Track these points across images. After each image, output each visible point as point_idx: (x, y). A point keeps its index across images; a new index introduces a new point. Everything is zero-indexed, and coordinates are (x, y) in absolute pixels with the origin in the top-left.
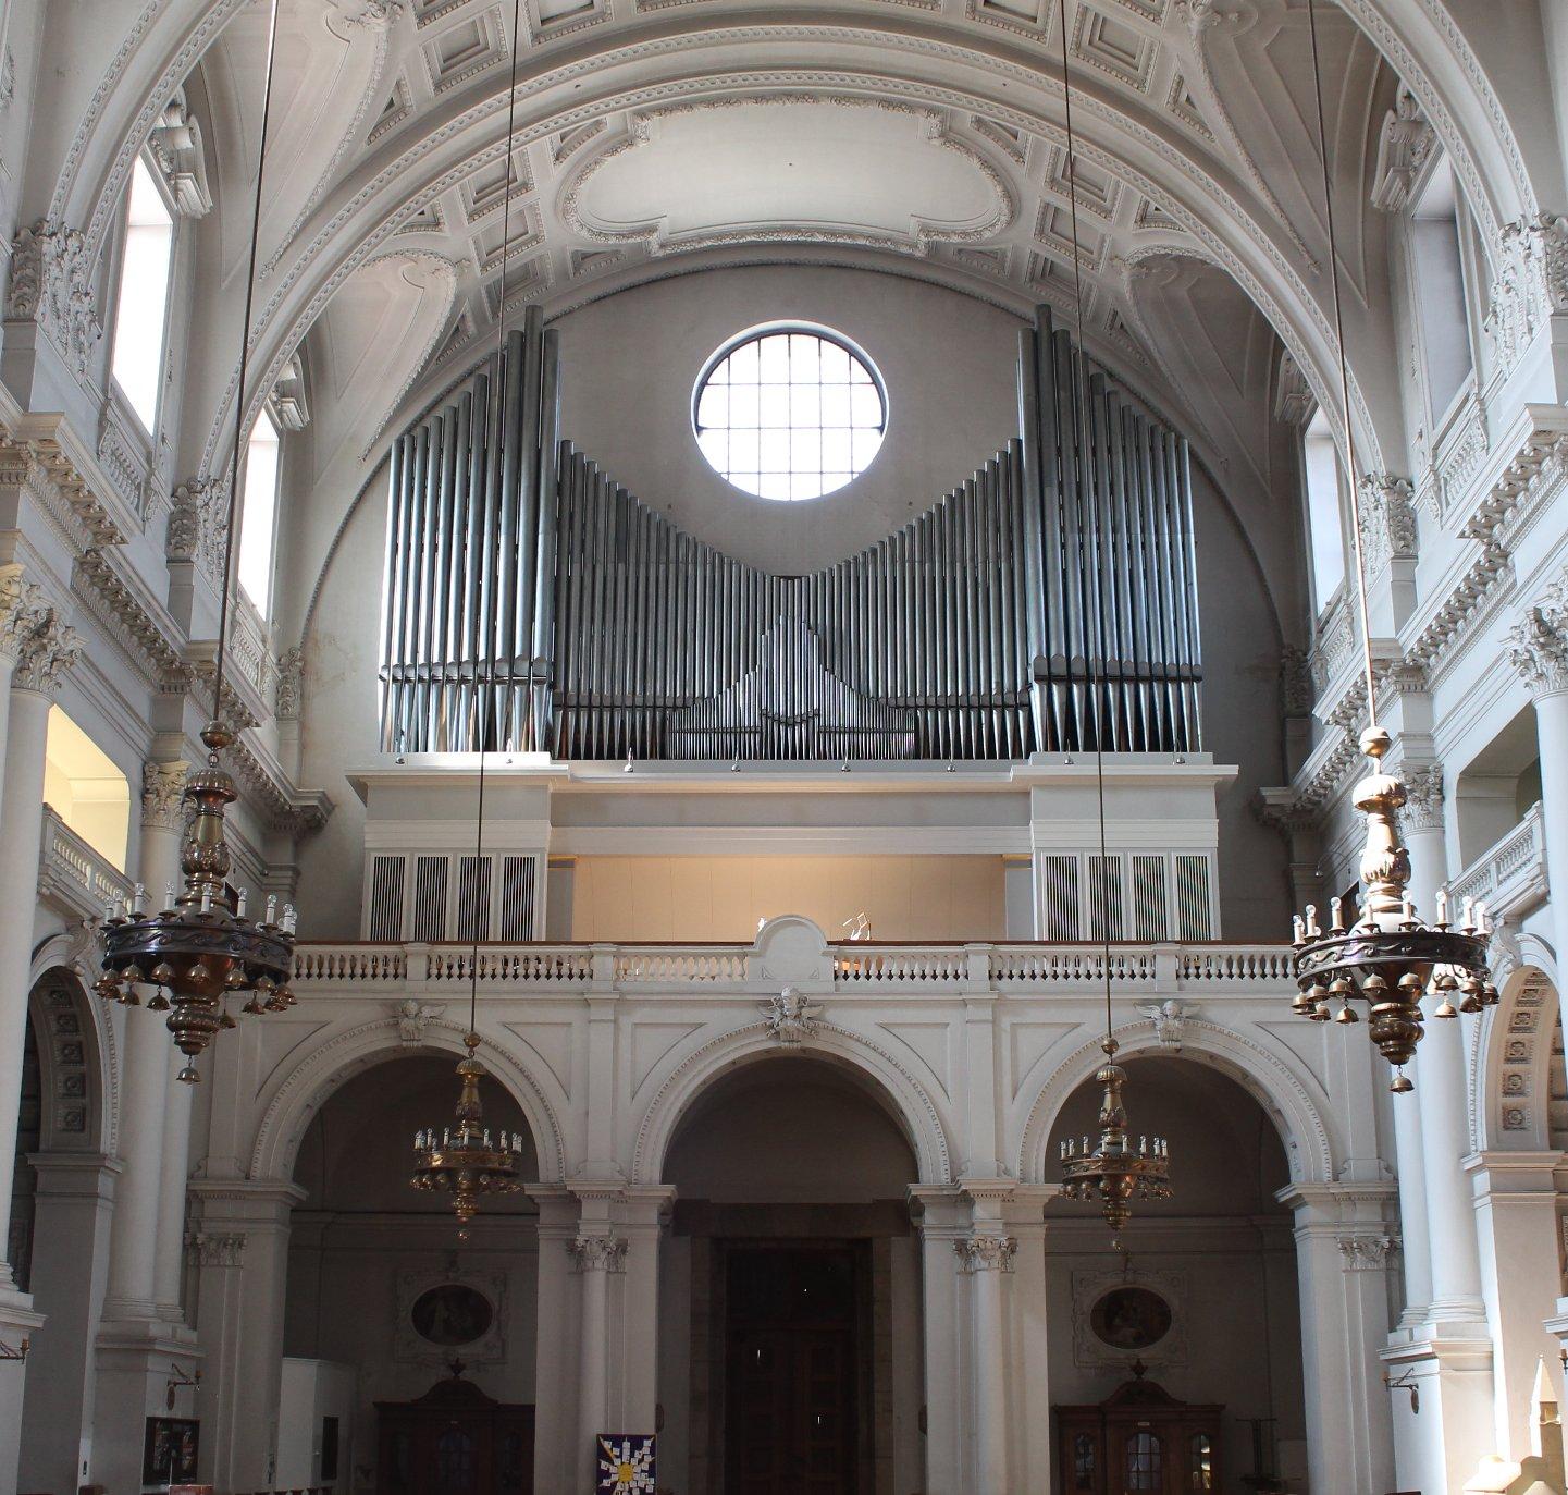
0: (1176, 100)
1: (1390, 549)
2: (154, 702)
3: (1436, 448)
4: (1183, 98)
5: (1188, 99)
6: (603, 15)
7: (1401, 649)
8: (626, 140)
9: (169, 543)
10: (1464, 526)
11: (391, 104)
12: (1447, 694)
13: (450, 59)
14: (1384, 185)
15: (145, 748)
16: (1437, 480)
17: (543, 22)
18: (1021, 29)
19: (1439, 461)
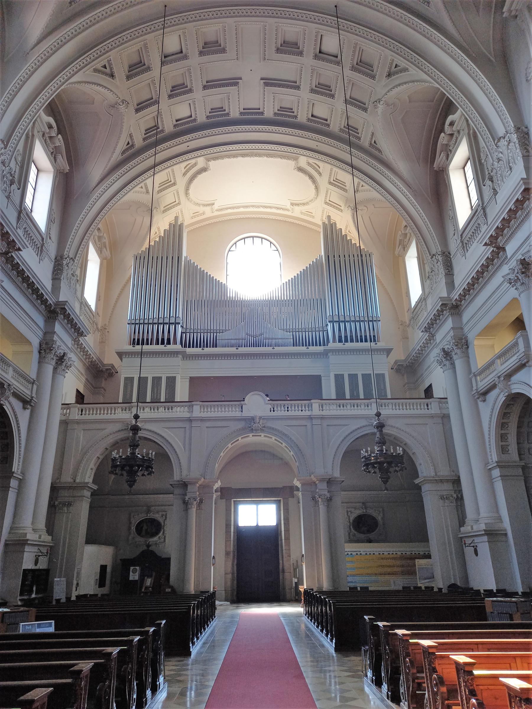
0: (371, 142)
1: (443, 273)
2: (45, 321)
3: (461, 235)
4: (373, 142)
5: (375, 142)
6: (195, 120)
7: (451, 300)
8: (204, 170)
9: (53, 273)
10: (486, 240)
11: (128, 143)
12: (466, 316)
13: (148, 131)
14: (440, 159)
15: (41, 336)
16: (463, 244)
17: (177, 121)
18: (322, 124)
19: (463, 238)
